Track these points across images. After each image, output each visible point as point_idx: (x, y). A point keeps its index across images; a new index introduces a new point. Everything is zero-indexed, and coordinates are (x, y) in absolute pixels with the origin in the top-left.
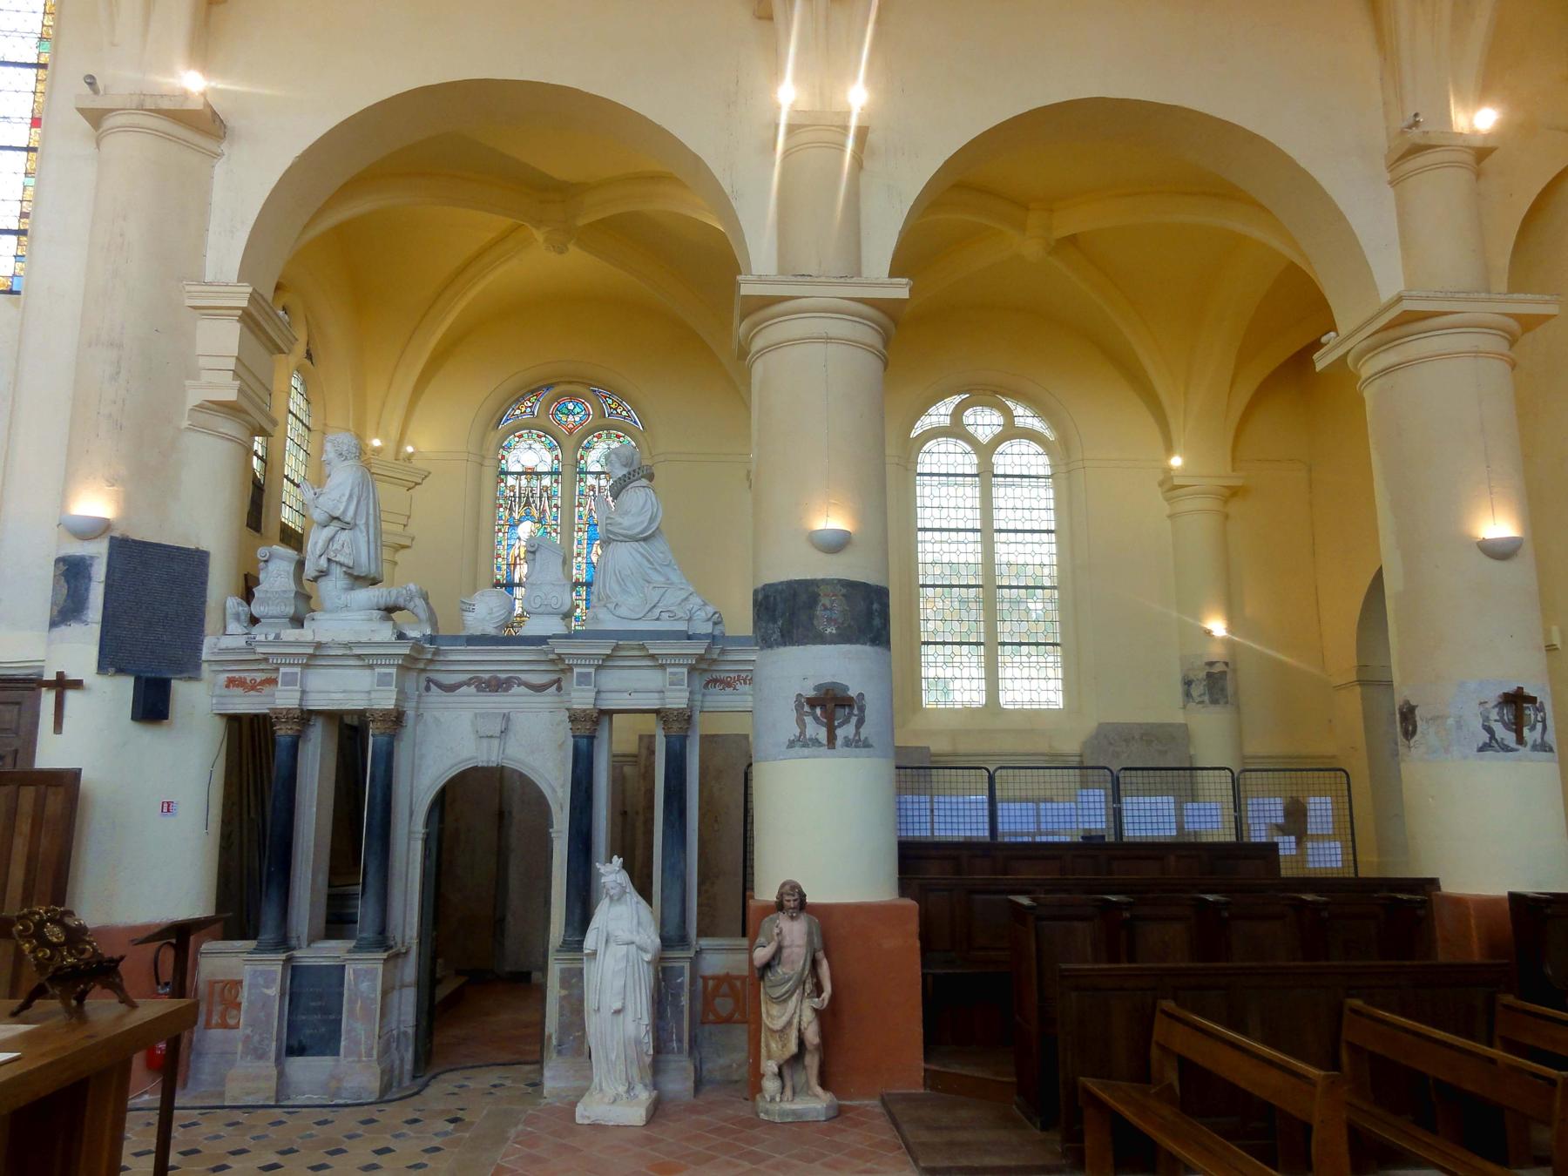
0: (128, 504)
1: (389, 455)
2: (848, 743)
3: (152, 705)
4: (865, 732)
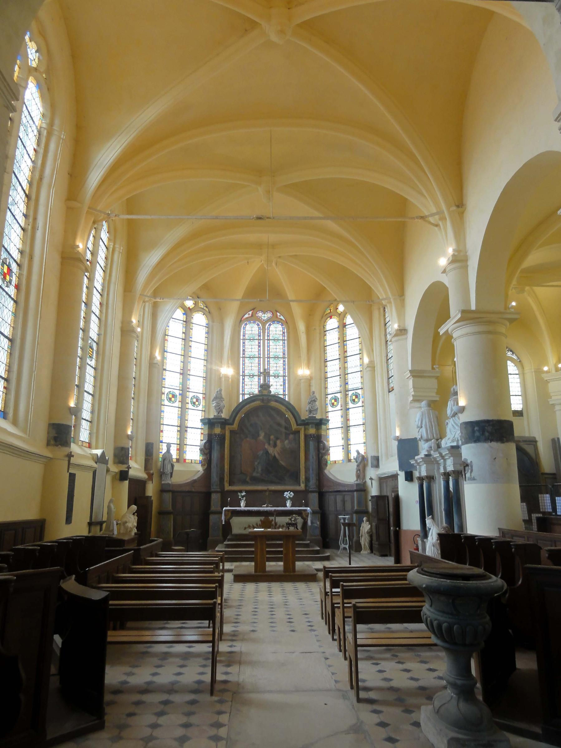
0: (401, 431)
1: (554, 371)
2: (468, 480)
3: (409, 477)
4: (473, 475)
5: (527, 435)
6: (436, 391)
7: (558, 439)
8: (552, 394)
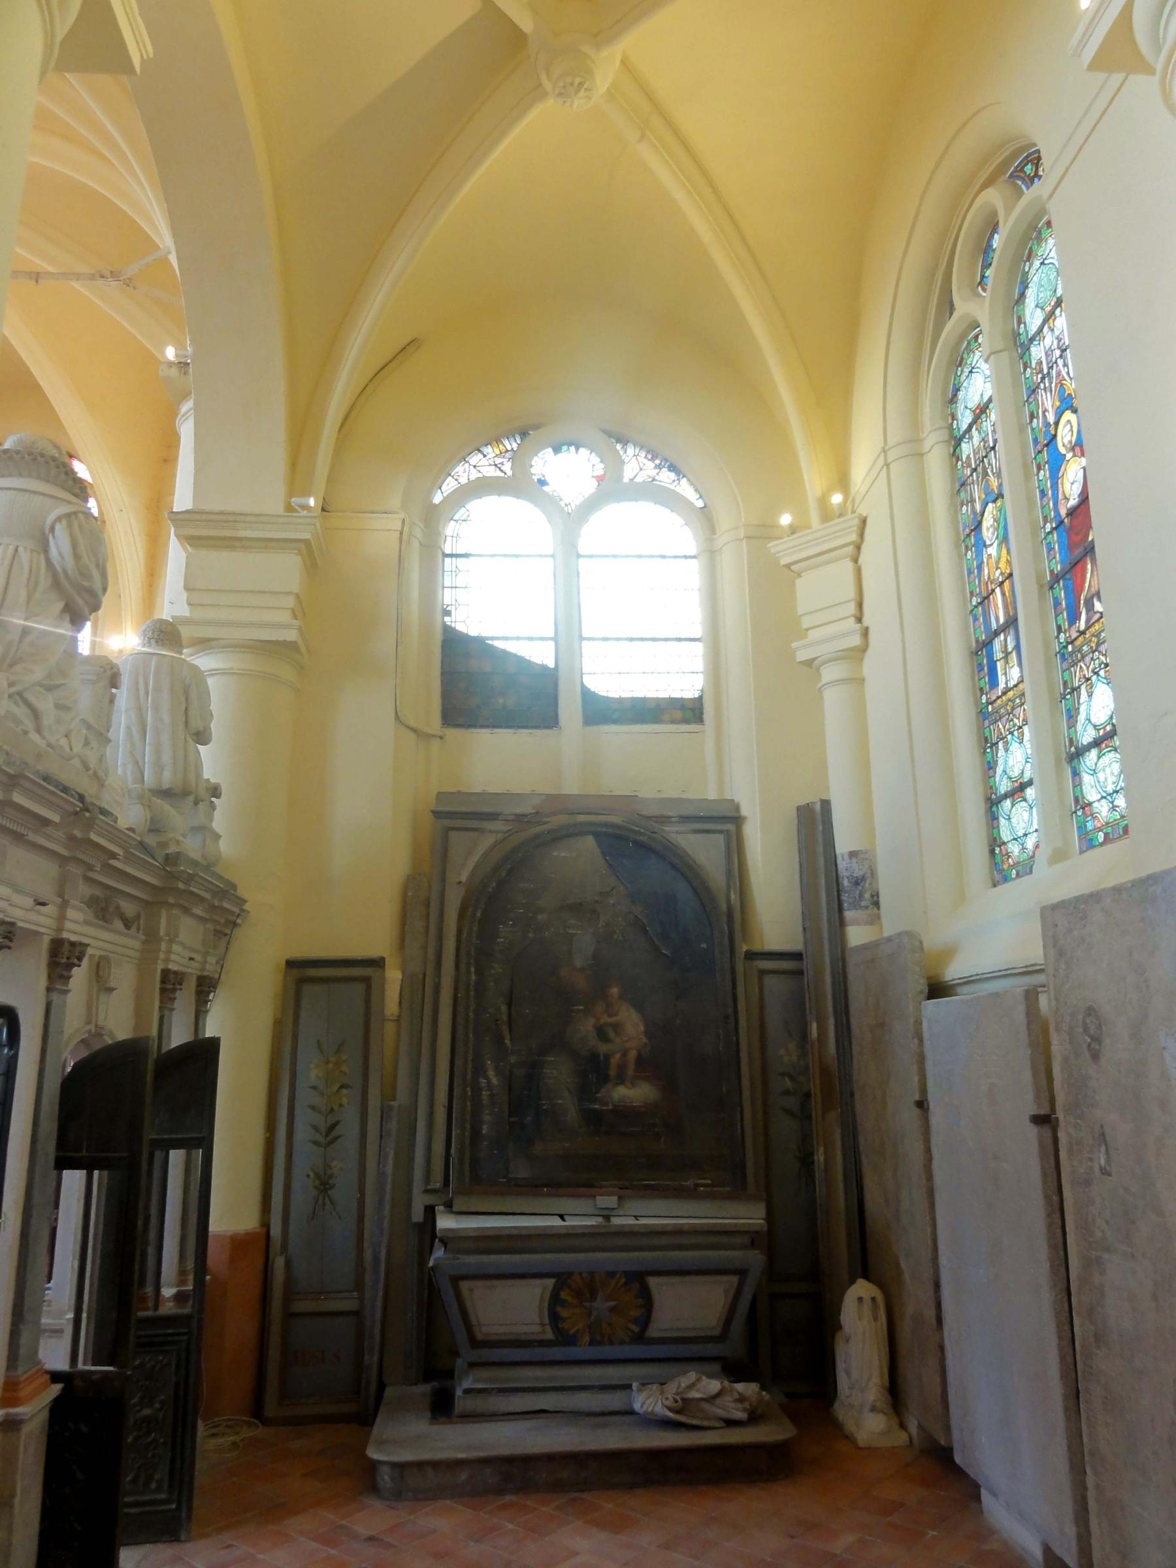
5: (712, 795)
6: (290, 602)
7: (826, 804)
8: (806, 622)
